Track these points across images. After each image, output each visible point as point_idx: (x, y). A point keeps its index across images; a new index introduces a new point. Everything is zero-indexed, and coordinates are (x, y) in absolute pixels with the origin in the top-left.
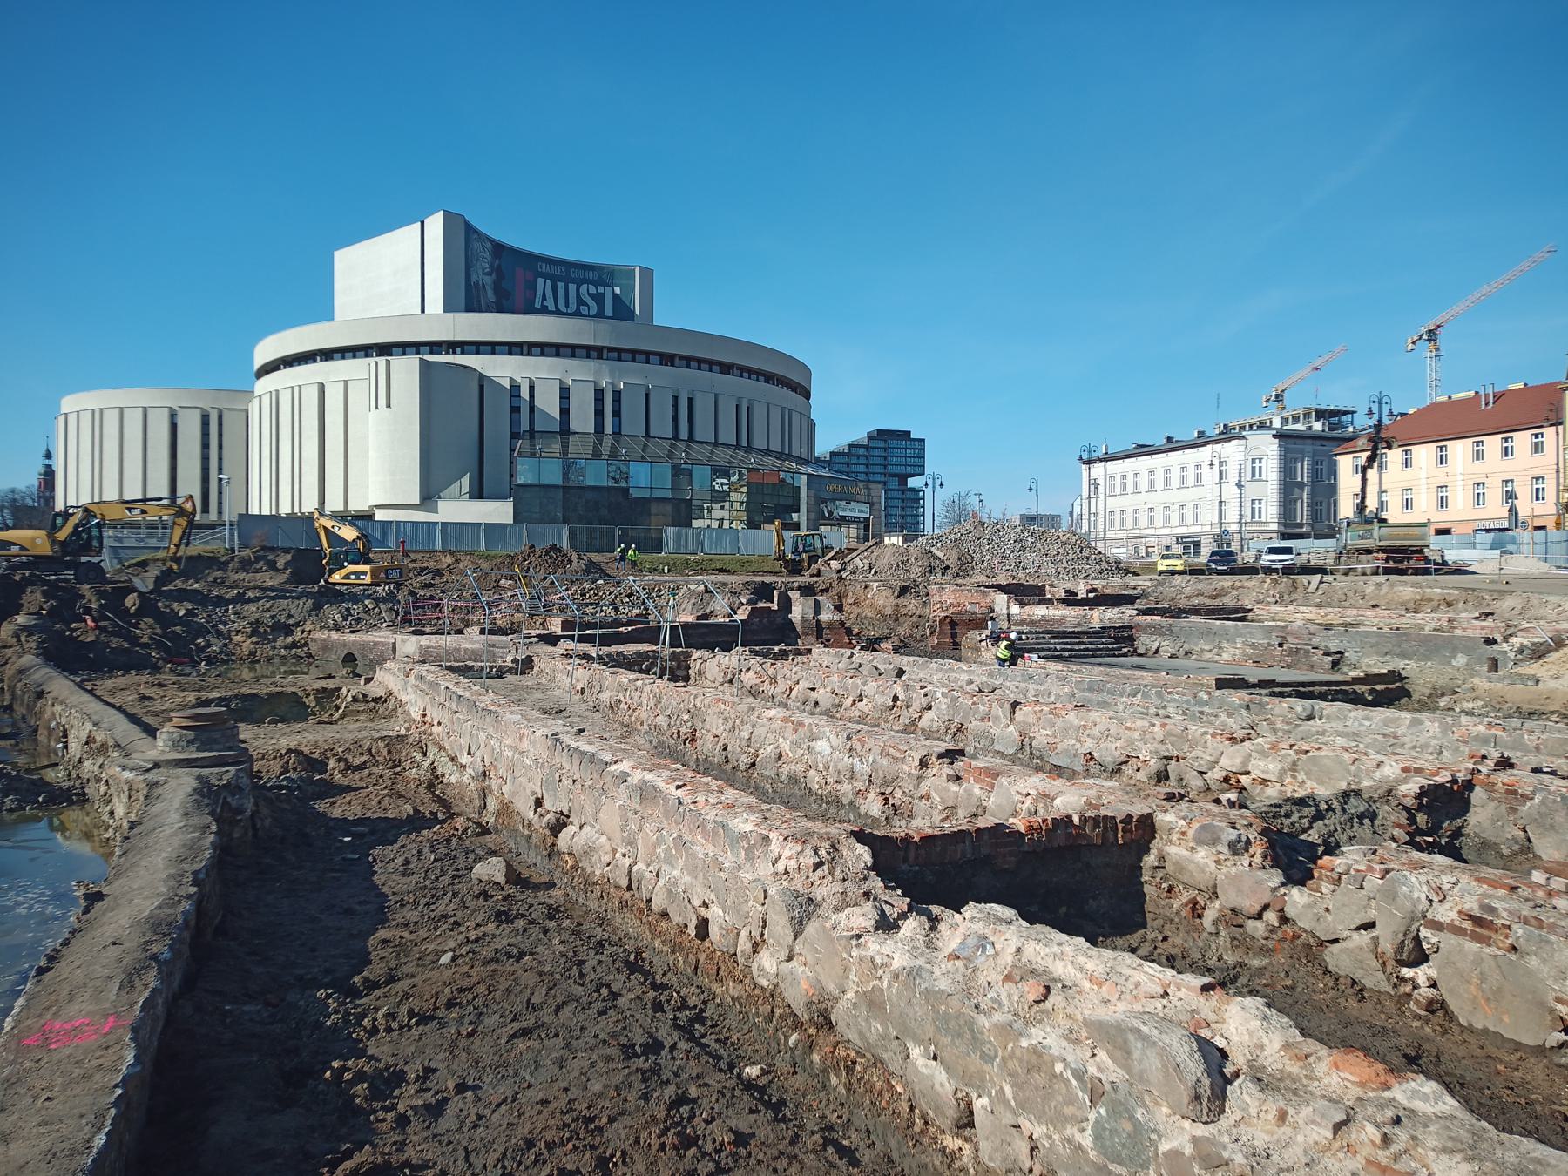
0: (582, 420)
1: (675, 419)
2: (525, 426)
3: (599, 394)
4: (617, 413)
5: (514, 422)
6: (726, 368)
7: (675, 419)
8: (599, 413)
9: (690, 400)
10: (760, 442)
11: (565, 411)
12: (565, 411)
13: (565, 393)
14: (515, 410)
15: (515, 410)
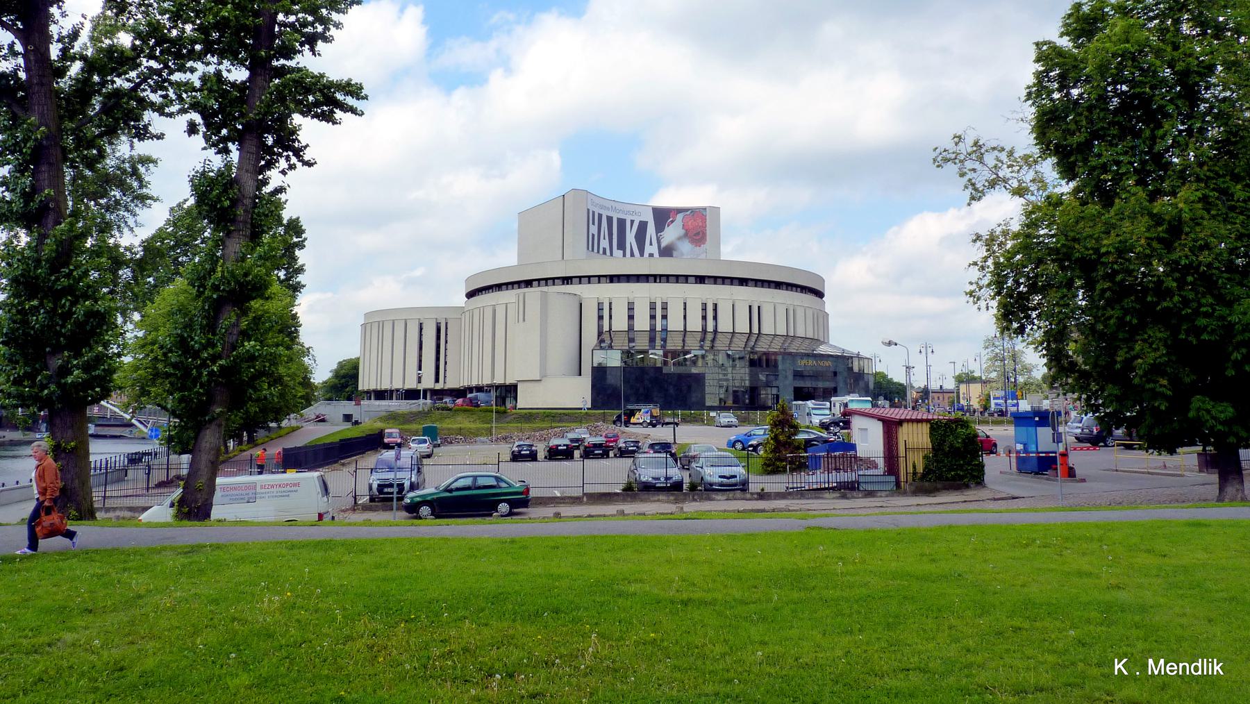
0: (642, 323)
1: (704, 318)
2: (606, 328)
3: (653, 307)
4: (664, 317)
5: (600, 327)
6: (743, 282)
7: (704, 318)
8: (653, 317)
9: (715, 305)
10: (767, 329)
11: (631, 317)
12: (631, 317)
13: (631, 308)
14: (601, 318)
15: (601, 318)
